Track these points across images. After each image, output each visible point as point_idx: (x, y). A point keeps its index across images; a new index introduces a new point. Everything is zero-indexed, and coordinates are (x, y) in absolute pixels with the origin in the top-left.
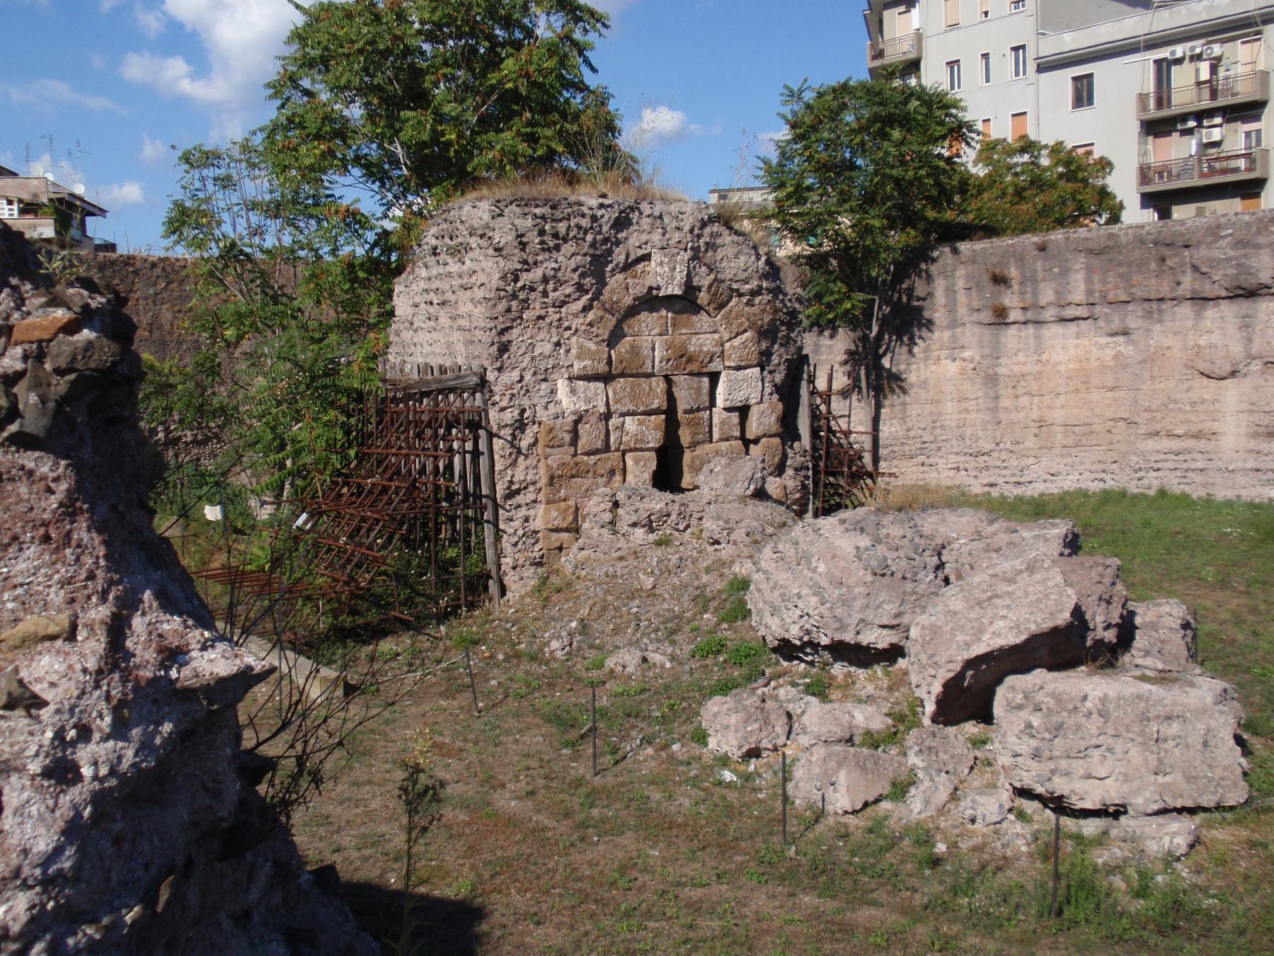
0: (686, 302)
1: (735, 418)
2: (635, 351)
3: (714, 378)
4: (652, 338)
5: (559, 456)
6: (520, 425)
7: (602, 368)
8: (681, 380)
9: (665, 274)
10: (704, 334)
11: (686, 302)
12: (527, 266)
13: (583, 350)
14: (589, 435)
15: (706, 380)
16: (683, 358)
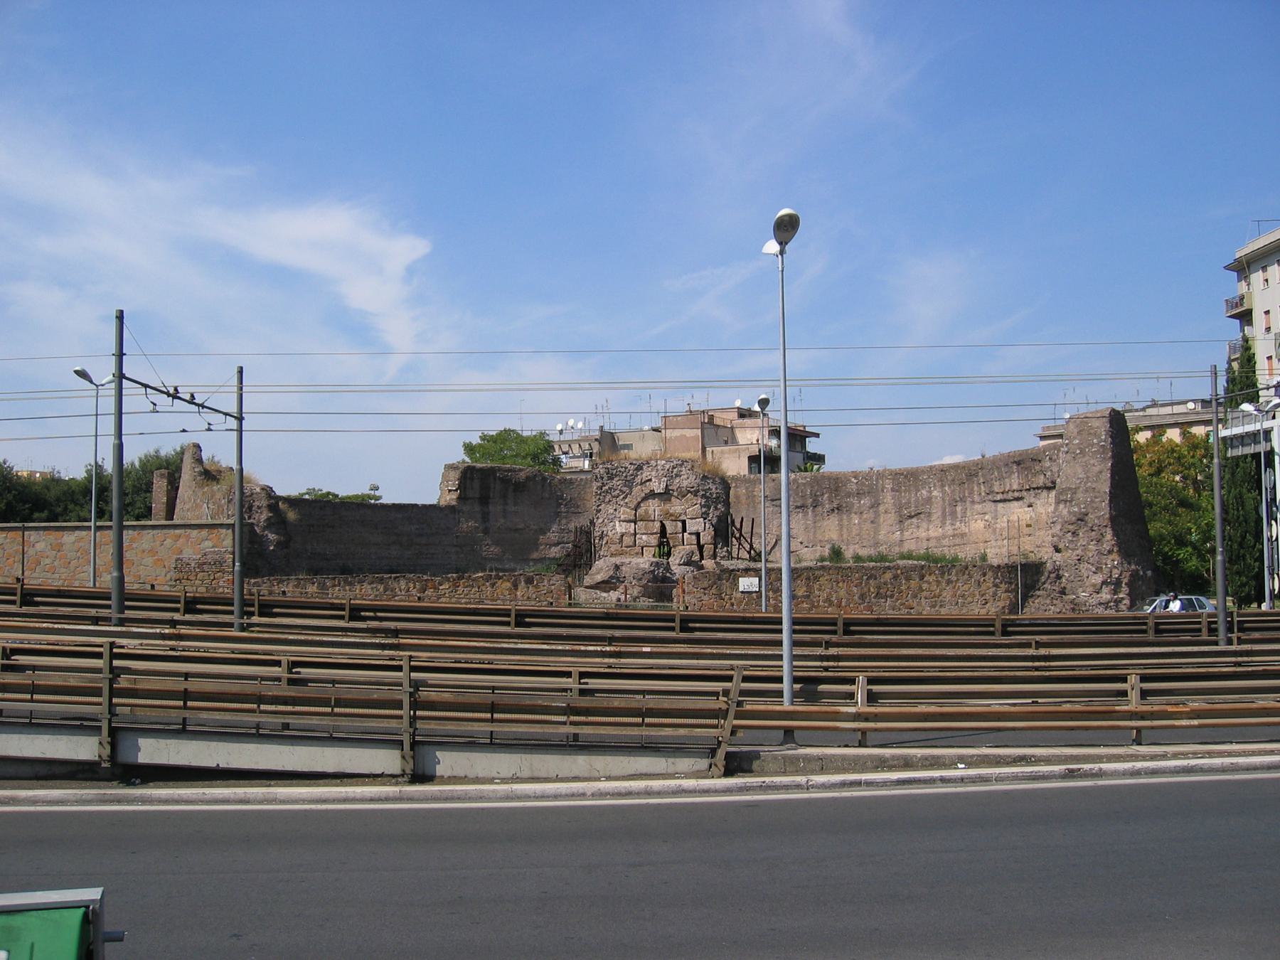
0: (666, 495)
1: (694, 537)
2: (647, 512)
3: (684, 522)
4: (654, 507)
5: (613, 548)
6: (601, 538)
7: (632, 517)
8: (667, 523)
9: (658, 487)
10: (676, 507)
11: (666, 495)
12: (604, 485)
13: (626, 513)
14: (628, 540)
15: (680, 524)
16: (668, 515)
